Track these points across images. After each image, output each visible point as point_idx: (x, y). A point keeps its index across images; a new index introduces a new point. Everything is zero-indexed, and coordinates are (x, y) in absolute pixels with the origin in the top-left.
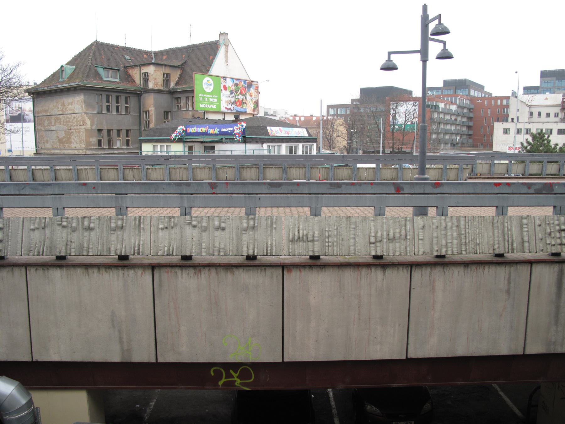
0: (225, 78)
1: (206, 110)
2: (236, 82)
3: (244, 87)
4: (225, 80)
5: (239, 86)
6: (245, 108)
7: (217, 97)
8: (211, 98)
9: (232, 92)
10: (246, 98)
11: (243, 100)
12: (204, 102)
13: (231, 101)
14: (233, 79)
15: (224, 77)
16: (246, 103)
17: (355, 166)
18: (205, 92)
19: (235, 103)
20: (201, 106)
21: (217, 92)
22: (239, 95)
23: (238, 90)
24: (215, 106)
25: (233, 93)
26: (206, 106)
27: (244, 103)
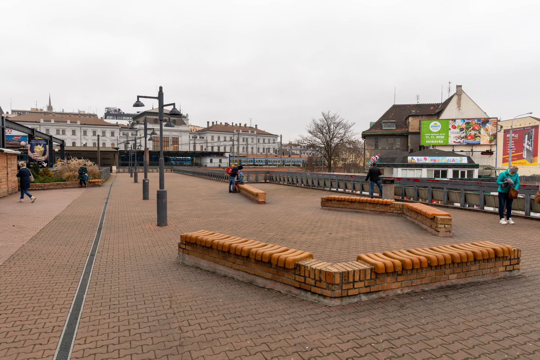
0: (454, 120)
1: (434, 144)
2: (466, 121)
3: (478, 124)
4: (455, 121)
5: (471, 124)
6: (478, 140)
7: (444, 134)
8: (438, 136)
9: (462, 130)
10: (480, 133)
11: (475, 134)
12: (431, 139)
13: (460, 136)
14: (463, 119)
15: (452, 120)
16: (479, 137)
17: (476, 180)
18: (431, 132)
19: (466, 137)
20: (427, 142)
21: (445, 130)
22: (470, 131)
23: (470, 128)
24: (442, 142)
25: (464, 130)
26: (433, 142)
27: (476, 137)
